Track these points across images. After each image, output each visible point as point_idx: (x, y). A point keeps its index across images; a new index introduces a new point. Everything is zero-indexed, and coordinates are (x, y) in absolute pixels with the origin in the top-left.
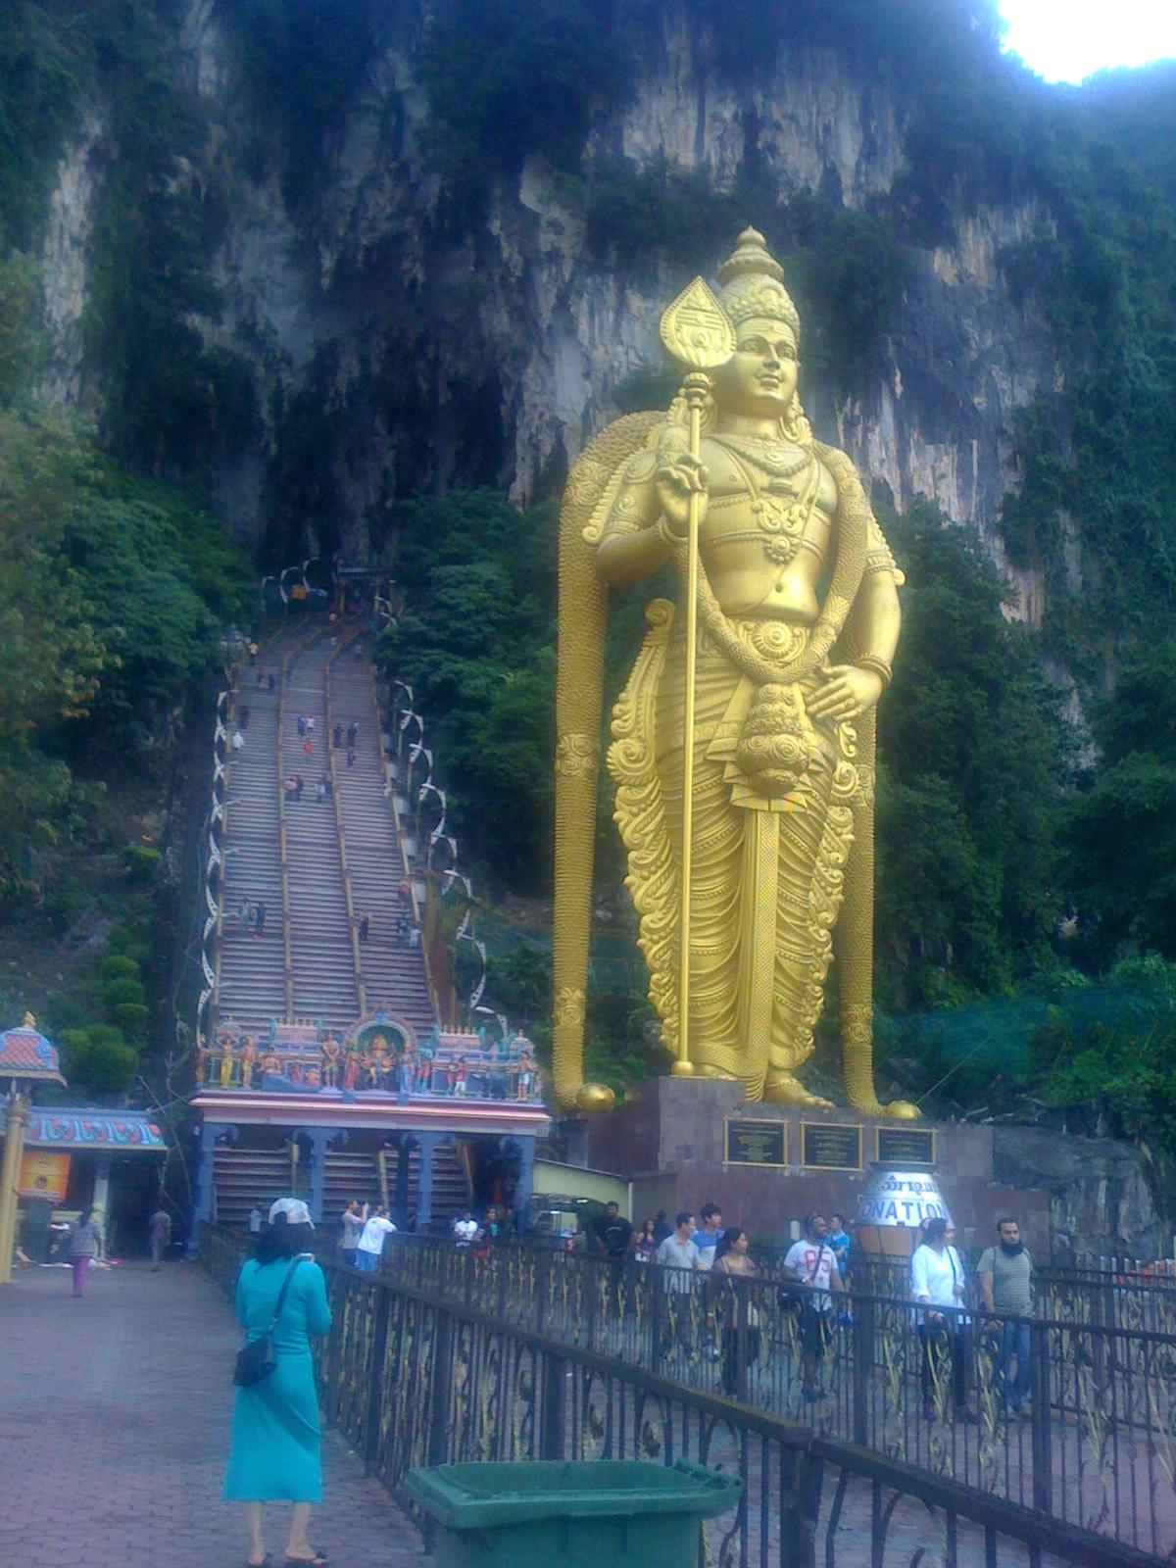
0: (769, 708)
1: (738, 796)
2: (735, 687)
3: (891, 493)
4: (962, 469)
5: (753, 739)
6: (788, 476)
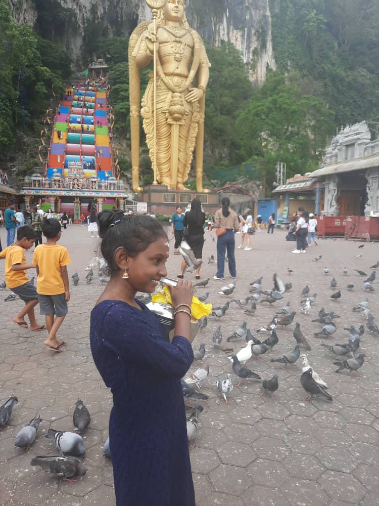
0: (175, 98)
1: (170, 121)
2: (168, 94)
4: (243, 36)
5: (171, 107)
6: (179, 38)
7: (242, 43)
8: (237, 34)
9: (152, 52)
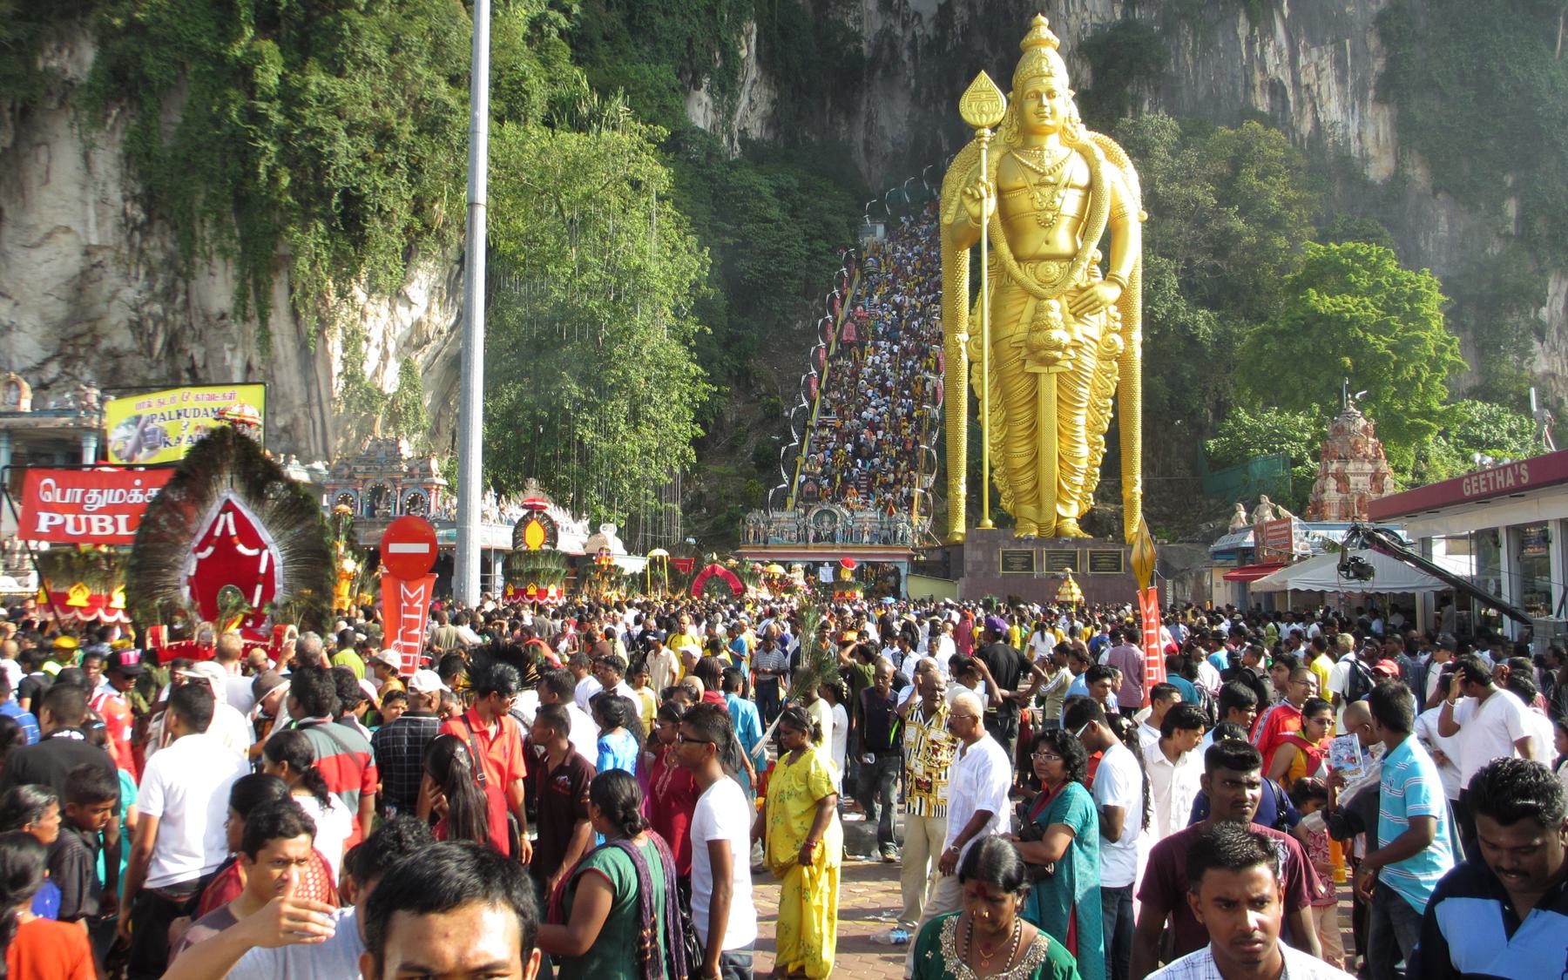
1: (1031, 367)
3: (1284, 88)
4: (1339, 63)
7: (1341, 80)
8: (1321, 57)
9: (978, 220)
